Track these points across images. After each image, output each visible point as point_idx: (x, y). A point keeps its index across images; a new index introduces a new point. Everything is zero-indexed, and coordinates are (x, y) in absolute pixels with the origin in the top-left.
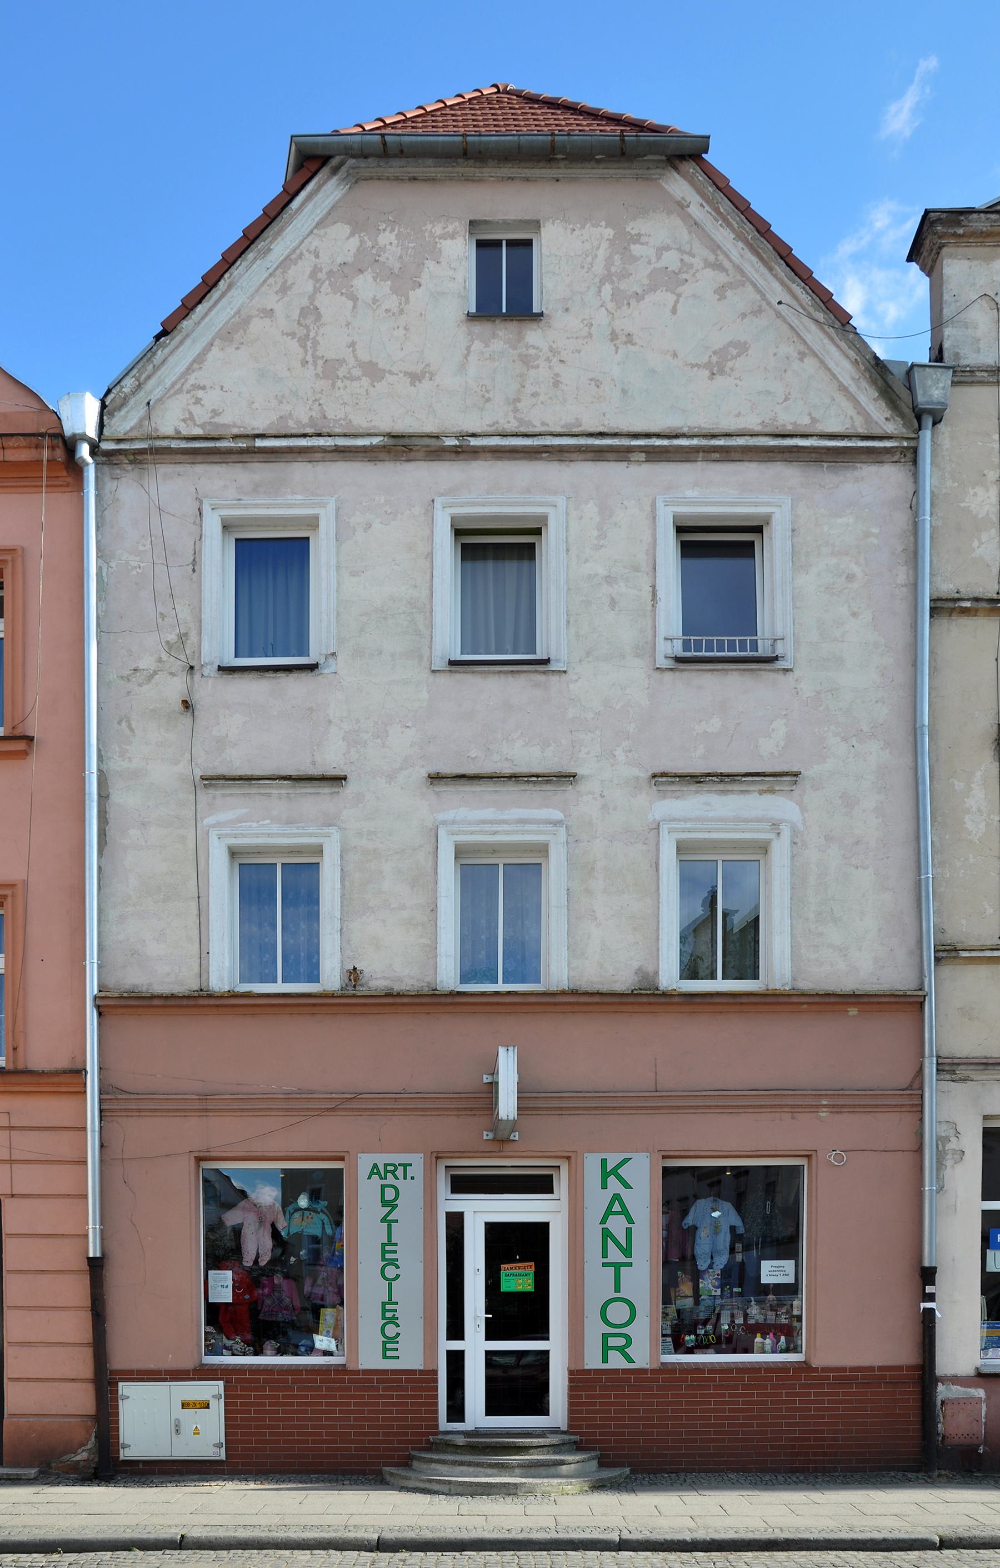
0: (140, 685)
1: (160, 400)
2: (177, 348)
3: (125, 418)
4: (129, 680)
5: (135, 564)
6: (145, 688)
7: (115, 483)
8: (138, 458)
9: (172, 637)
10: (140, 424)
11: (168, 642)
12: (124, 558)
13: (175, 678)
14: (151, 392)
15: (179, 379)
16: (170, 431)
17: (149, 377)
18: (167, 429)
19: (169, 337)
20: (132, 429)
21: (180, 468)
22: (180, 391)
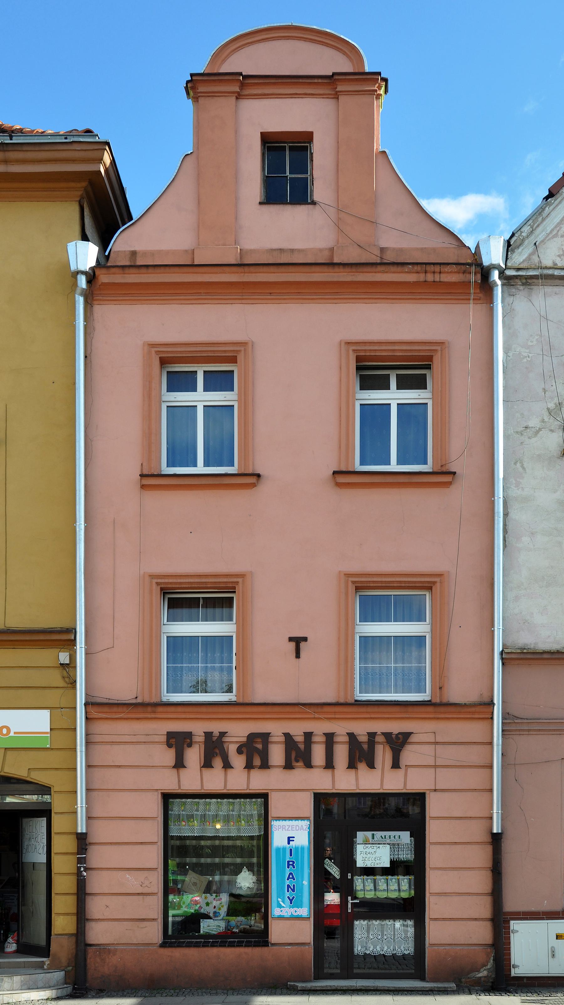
0: (529, 438)
1: (542, 241)
2: (557, 206)
3: (520, 254)
4: (522, 434)
5: (526, 354)
6: (534, 440)
7: (512, 298)
8: (528, 281)
9: (551, 405)
10: (529, 258)
11: (548, 409)
12: (518, 350)
13: (554, 434)
14: (538, 235)
15: (556, 227)
16: (549, 263)
17: (538, 226)
18: (547, 262)
19: (553, 198)
20: (524, 261)
21: (556, 289)
22: (556, 236)
